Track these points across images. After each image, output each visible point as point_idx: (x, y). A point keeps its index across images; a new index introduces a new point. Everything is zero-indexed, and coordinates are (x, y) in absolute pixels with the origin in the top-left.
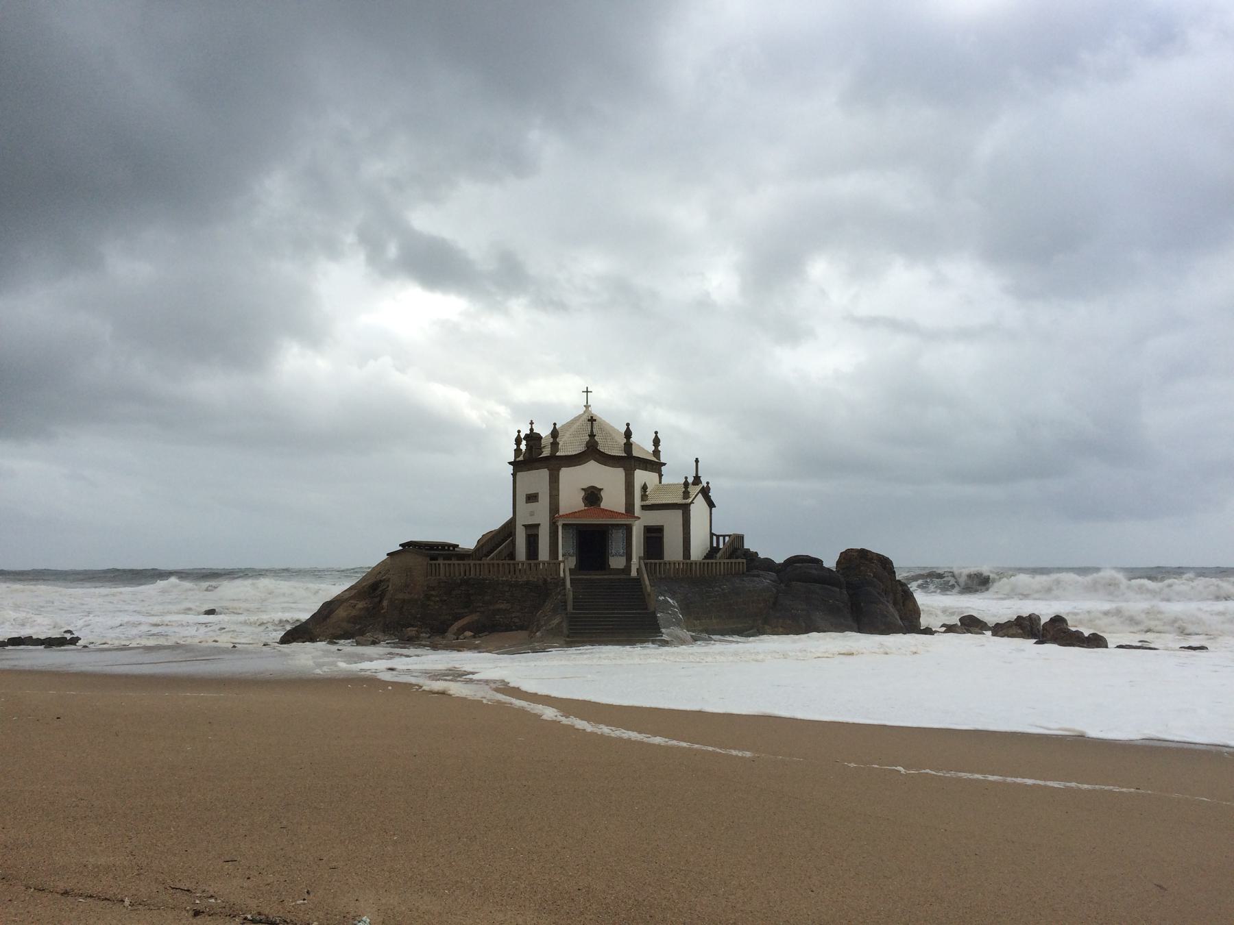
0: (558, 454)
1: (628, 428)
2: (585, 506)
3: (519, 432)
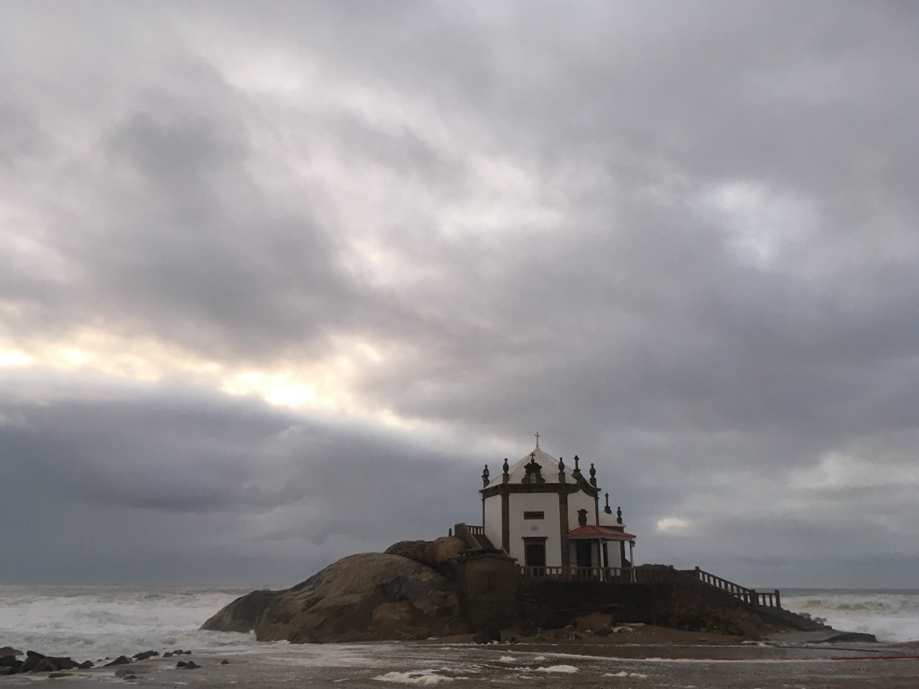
0: (567, 482)
1: (592, 467)
2: (580, 524)
3: (506, 460)
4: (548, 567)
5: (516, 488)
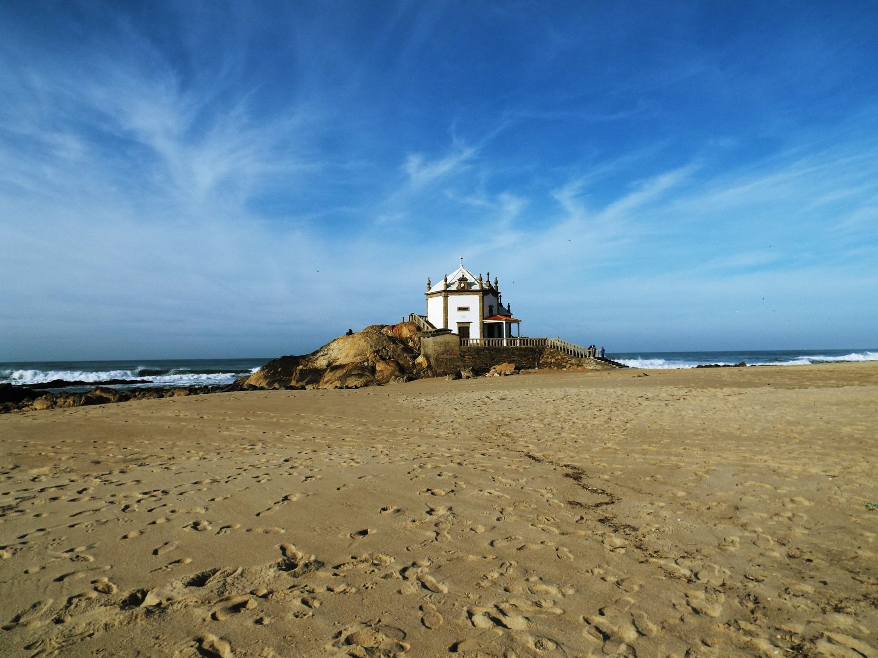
4: (473, 340)
5: (452, 292)
